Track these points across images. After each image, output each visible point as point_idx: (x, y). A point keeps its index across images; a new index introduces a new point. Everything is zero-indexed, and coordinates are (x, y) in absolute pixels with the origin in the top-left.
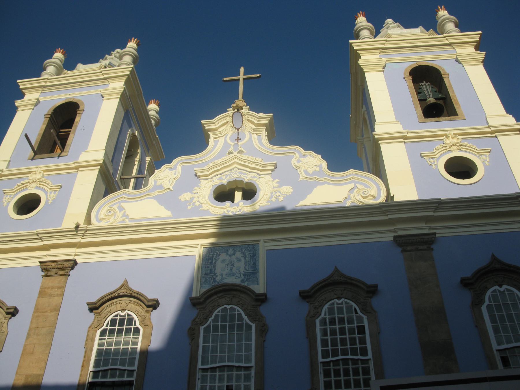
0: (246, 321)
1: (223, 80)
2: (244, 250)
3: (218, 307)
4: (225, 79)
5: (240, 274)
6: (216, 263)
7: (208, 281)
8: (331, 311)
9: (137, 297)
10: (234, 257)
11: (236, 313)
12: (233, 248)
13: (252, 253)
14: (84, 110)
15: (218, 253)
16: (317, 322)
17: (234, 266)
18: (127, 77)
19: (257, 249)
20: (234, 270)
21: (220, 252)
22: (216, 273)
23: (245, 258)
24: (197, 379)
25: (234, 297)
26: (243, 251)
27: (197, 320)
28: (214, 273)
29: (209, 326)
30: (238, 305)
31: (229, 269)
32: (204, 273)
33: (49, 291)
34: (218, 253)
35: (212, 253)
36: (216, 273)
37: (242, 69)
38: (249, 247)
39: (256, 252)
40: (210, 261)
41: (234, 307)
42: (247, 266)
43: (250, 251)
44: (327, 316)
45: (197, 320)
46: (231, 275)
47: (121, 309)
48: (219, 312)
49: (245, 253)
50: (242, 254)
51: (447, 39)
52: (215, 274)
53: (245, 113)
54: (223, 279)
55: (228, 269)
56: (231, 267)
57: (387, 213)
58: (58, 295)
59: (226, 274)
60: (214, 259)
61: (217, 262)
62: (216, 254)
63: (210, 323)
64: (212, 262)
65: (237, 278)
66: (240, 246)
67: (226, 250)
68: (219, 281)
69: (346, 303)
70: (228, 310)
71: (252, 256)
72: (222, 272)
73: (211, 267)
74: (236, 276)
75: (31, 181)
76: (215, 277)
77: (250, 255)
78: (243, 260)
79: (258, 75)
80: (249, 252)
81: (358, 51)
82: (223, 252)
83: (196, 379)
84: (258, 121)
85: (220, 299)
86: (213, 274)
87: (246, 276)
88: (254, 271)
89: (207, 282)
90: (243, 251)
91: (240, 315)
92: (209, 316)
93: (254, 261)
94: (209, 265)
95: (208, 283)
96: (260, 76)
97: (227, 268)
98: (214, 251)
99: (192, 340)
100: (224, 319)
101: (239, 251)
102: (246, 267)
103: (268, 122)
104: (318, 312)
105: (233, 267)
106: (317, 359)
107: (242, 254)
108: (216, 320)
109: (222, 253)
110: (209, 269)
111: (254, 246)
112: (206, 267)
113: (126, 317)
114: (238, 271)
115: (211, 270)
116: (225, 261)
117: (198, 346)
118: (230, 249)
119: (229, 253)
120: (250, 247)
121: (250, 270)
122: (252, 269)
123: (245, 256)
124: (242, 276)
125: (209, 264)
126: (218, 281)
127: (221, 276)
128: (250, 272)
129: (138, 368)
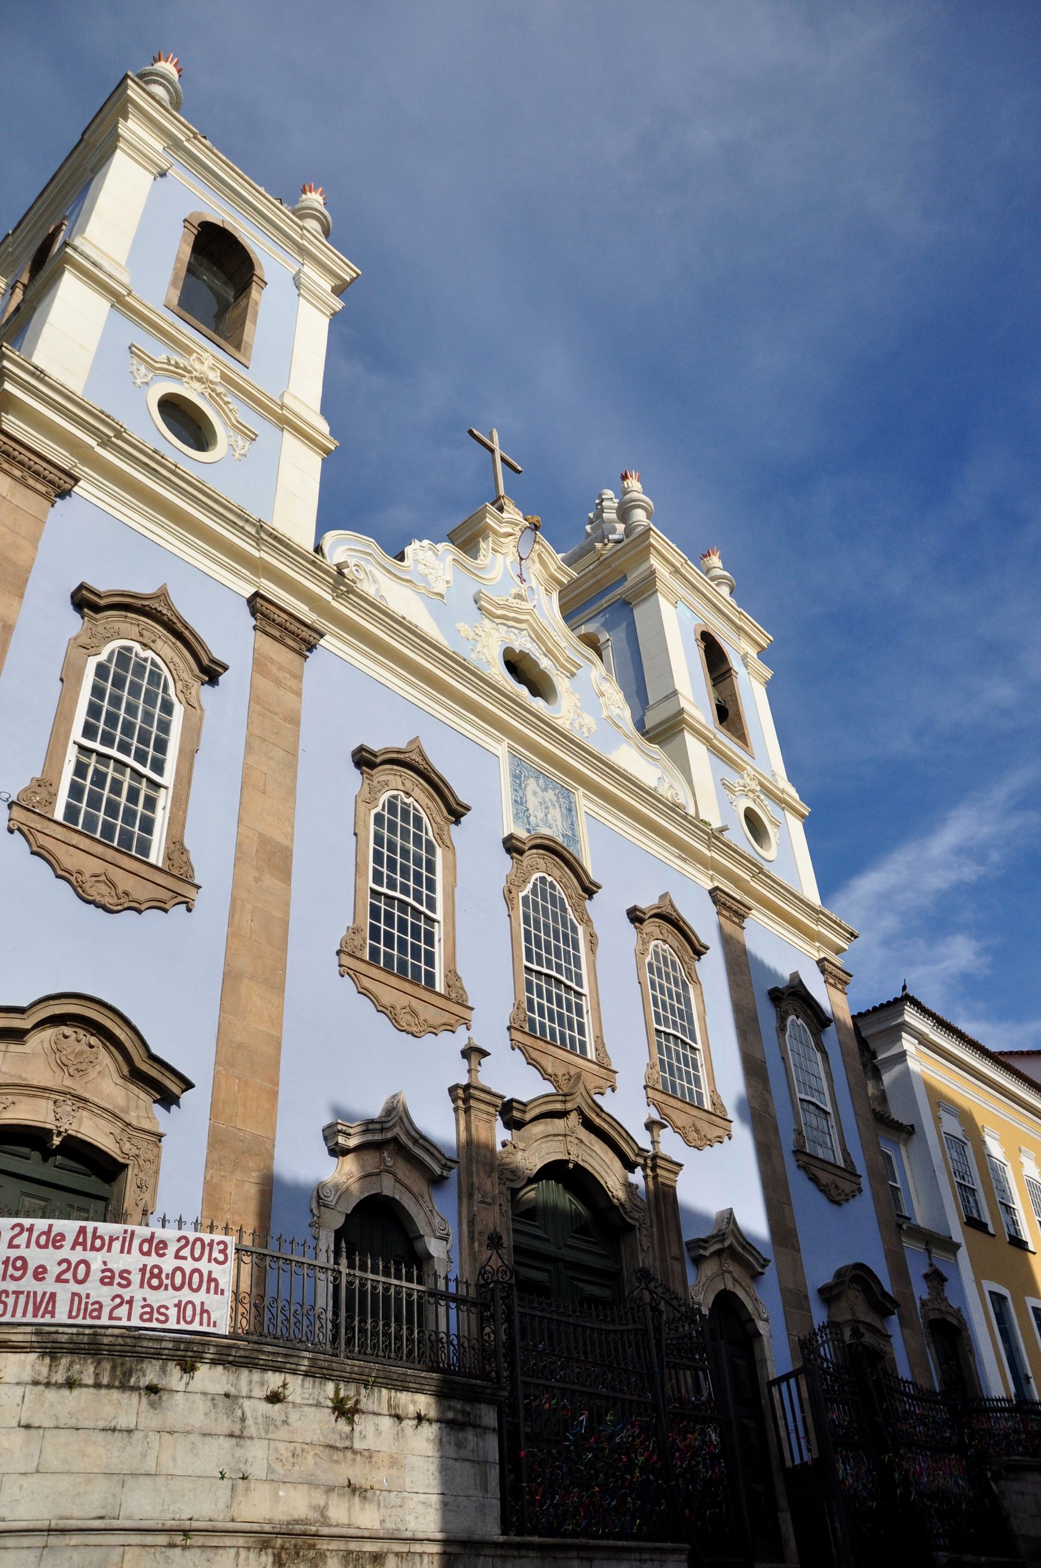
1: (471, 432)
4: (476, 432)
23: (560, 807)
33: (274, 669)
48: (536, 880)
58: (292, 691)
64: (520, 785)
75: (195, 374)
79: (520, 468)
84: (555, 570)
96: (519, 472)
108: (534, 891)
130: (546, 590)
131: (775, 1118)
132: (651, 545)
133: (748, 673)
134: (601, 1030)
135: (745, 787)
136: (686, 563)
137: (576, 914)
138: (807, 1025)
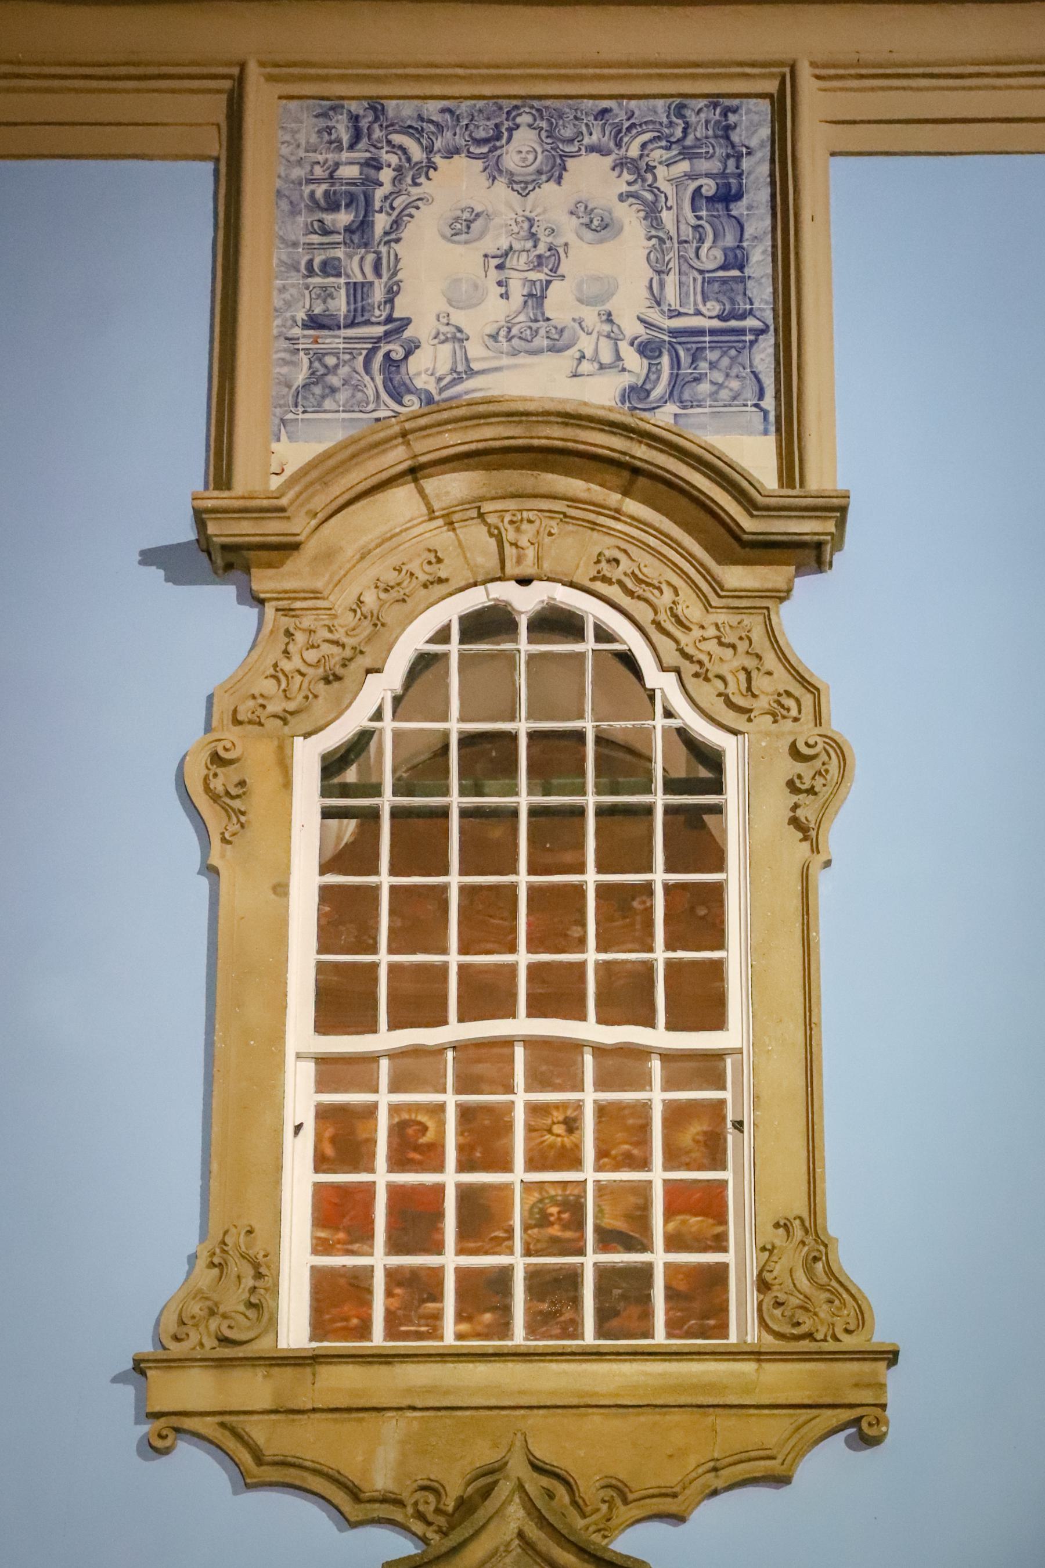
0: (668, 714)
2: (644, 146)
3: (439, 590)
6: (397, 241)
7: (334, 380)
12: (544, 124)
13: (708, 175)
15: (417, 153)
17: (554, 270)
19: (754, 143)
21: (429, 150)
22: (407, 322)
23: (652, 214)
24: (289, 1130)
26: (634, 151)
28: (389, 320)
31: (517, 290)
32: (301, 315)
34: (417, 153)
36: (407, 322)
38: (682, 116)
39: (745, 164)
40: (344, 218)
42: (671, 280)
43: (687, 154)
46: (540, 341)
48: (442, 636)
49: (650, 169)
50: (631, 178)
52: (397, 326)
54: (471, 373)
55: (505, 296)
56: (534, 276)
59: (494, 337)
60: (377, 205)
61: (407, 233)
62: (394, 160)
64: (361, 229)
65: (586, 367)
66: (605, 111)
67: (481, 134)
68: (432, 388)
71: (709, 199)
72: (459, 318)
74: (574, 352)
76: (398, 353)
80: (684, 166)
82: (457, 151)
83: (279, 1132)
86: (379, 330)
87: (665, 360)
88: (733, 323)
89: (333, 390)
90: (634, 151)
92: (367, 661)
93: (730, 240)
94: (340, 253)
95: (342, 396)
97: (500, 284)
98: (377, 133)
101: (602, 151)
102: (662, 285)
105: (549, 282)
107: (627, 176)
109: (451, 153)
110: (342, 280)
111: (725, 115)
112: (310, 263)
114: (590, 316)
115: (358, 291)
116: (475, 226)
117: (281, 889)
118: (518, 126)
119: (511, 160)
120: (692, 119)
121: (698, 313)
122: (713, 307)
123: (649, 197)
124: (633, 360)
125: (339, 238)
126: (424, 382)
127: (447, 347)
128: (701, 332)
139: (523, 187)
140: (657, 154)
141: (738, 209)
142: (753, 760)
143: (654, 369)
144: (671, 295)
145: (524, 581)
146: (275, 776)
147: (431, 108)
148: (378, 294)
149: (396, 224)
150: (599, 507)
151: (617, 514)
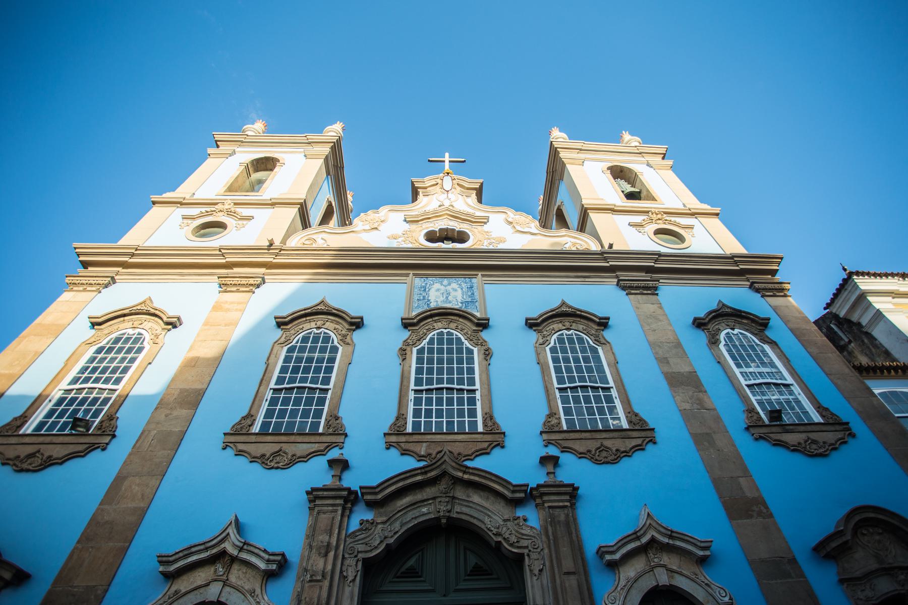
1: (429, 161)
4: (431, 159)
5: (457, 302)
8: (560, 340)
9: (336, 314)
10: (449, 288)
11: (454, 337)
14: (284, 164)
15: (432, 283)
16: (548, 349)
18: (333, 144)
20: (450, 298)
23: (462, 289)
25: (451, 322)
26: (459, 283)
27: (409, 341)
29: (423, 348)
30: (456, 330)
31: (445, 297)
35: (425, 282)
37: (447, 155)
40: (422, 289)
41: (452, 331)
43: (466, 283)
44: (558, 345)
45: (409, 341)
47: (316, 326)
48: (434, 335)
51: (638, 149)
52: (429, 300)
53: (456, 178)
57: (608, 260)
63: (425, 345)
64: (425, 290)
69: (576, 334)
70: (445, 334)
73: (424, 294)
77: (467, 287)
78: (459, 290)
79: (463, 160)
80: (466, 285)
81: (558, 149)
83: (408, 400)
85: (436, 322)
90: (459, 283)
91: (458, 339)
96: (465, 161)
99: (404, 360)
100: (441, 341)
103: (478, 187)
104: (547, 340)
106: (552, 384)
108: (431, 342)
109: (436, 283)
113: (322, 335)
114: (454, 300)
117: (410, 367)
119: (444, 284)
124: (460, 305)
129: (334, 386)
130: (466, 196)
131: (715, 409)
132: (556, 148)
133: (654, 169)
134: (491, 407)
135: (652, 220)
136: (584, 144)
137: (471, 342)
138: (747, 330)
139: (445, 286)
140: (462, 283)
141: (473, 289)
142: (479, 351)
143: (463, 305)
144: (465, 297)
145: (446, 329)
146: (410, 352)
147: (434, 279)
148: (427, 297)
149: (429, 290)
150: (456, 320)
151: (458, 321)
